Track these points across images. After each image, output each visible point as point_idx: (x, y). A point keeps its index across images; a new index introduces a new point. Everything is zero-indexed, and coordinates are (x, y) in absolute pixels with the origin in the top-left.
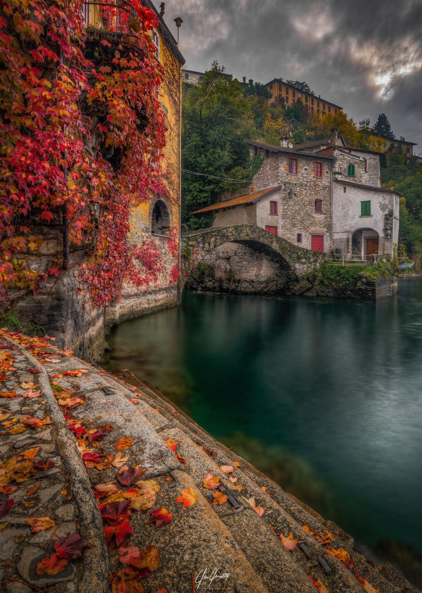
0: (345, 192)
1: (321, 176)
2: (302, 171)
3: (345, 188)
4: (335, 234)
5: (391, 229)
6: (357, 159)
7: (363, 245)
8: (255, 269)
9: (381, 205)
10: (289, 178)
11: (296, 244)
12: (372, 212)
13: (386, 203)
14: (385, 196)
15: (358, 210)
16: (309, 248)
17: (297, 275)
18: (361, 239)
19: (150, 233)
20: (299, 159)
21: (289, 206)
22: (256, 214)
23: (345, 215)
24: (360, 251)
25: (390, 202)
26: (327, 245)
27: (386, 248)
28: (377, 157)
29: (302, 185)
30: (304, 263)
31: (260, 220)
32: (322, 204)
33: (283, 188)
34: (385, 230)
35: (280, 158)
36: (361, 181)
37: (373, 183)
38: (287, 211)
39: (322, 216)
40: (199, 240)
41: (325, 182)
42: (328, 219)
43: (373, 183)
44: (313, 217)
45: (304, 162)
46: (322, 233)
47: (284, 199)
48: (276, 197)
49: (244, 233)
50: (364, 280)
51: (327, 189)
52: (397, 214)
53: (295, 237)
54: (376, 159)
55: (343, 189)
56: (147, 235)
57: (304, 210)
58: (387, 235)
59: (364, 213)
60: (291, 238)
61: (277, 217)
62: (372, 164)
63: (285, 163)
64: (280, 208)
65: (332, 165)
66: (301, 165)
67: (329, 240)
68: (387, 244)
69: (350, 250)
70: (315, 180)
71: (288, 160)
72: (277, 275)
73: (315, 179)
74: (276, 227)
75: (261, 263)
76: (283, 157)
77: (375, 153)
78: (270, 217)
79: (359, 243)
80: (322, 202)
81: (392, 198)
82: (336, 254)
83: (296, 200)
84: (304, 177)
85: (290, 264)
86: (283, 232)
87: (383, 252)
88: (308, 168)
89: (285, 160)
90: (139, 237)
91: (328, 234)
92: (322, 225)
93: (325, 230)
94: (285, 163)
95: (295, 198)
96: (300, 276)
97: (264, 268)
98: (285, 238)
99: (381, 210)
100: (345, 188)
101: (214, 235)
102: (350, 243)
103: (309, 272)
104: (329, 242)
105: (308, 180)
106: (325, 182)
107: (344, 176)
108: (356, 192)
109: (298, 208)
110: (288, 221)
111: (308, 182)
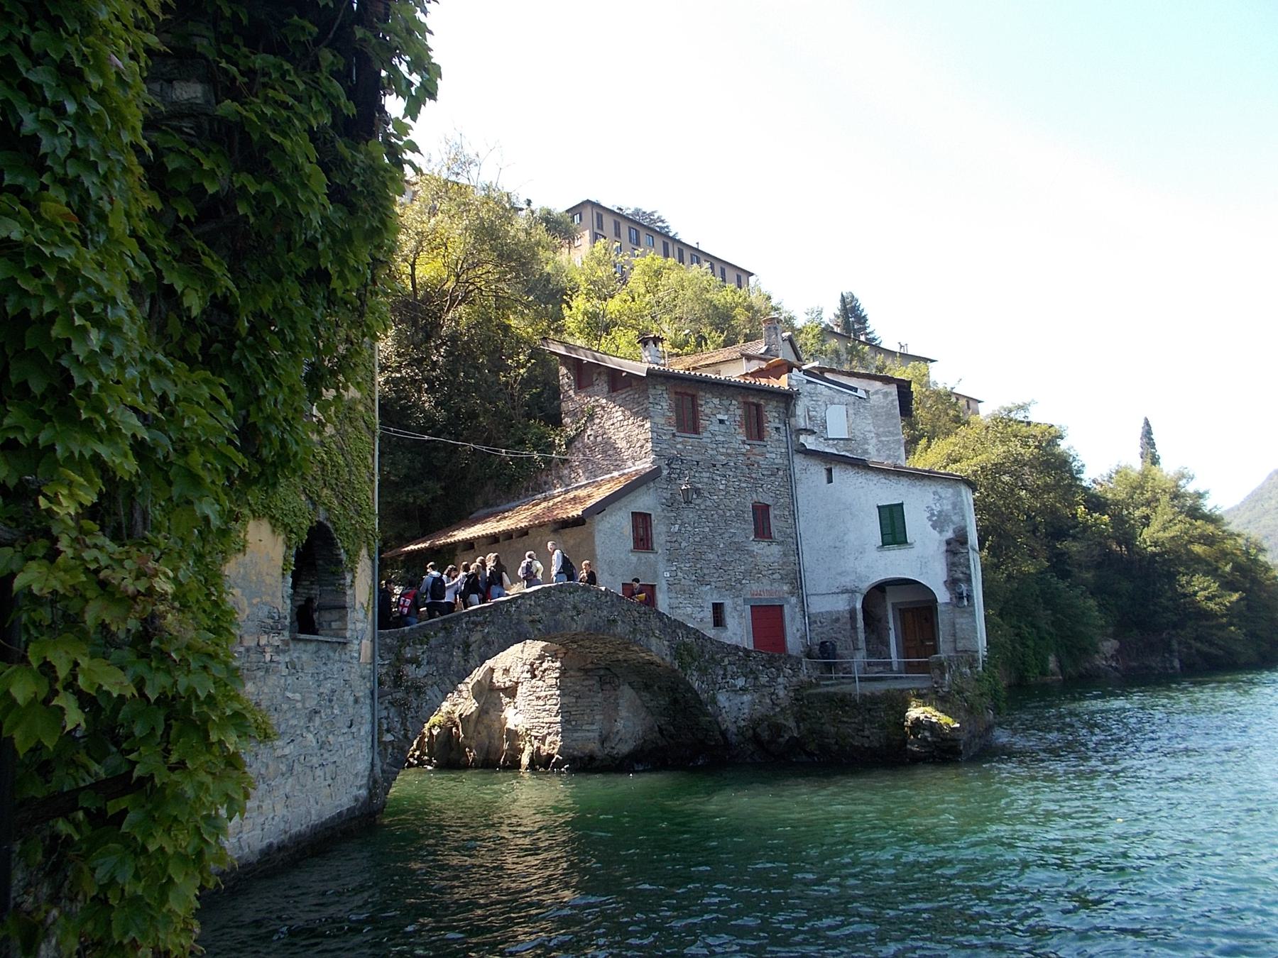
0: (830, 481)
1: (761, 438)
2: (711, 428)
3: (829, 471)
4: (812, 600)
5: (969, 580)
6: (850, 395)
7: (891, 625)
8: (597, 717)
9: (933, 515)
10: (679, 446)
11: (711, 632)
12: (911, 535)
13: (945, 508)
14: (939, 490)
15: (872, 529)
16: (748, 644)
17: (723, 727)
18: (886, 611)
19: (286, 633)
20: (702, 393)
21: (683, 524)
22: (594, 550)
23: (838, 544)
24: (888, 645)
25: (954, 506)
26: (794, 634)
27: (959, 634)
28: (893, 389)
29: (714, 466)
30: (744, 690)
31: (605, 567)
32: (771, 516)
33: (665, 472)
34: (952, 583)
35: (651, 391)
36: (865, 452)
37: (889, 457)
38: (680, 540)
39: (775, 549)
40: (433, 641)
41: (774, 456)
42: (792, 558)
43: (889, 457)
44: (750, 553)
45: (716, 401)
46: (780, 599)
47: (670, 504)
48: (644, 501)
49: (567, 610)
51: (781, 473)
52: (973, 538)
53: (708, 614)
54: (891, 393)
55: (824, 473)
56: (276, 641)
57: (726, 536)
58: (960, 597)
59: (889, 538)
60: (696, 615)
61: (651, 556)
62: (883, 407)
63: (664, 404)
64: (659, 532)
65: (787, 409)
66: (708, 411)
67: (799, 616)
68: (962, 621)
69: (862, 644)
70: (747, 450)
71: (673, 396)
72: (661, 730)
73: (748, 447)
74: (653, 587)
75: (616, 699)
76: (660, 389)
77: (888, 380)
78: (634, 558)
79: (879, 621)
80: (771, 510)
81: (959, 494)
82: (825, 654)
83: (703, 507)
84: (717, 443)
85: (704, 696)
86: (672, 601)
88: (725, 418)
89: (665, 396)
90: (248, 650)
91: (794, 600)
92: (776, 576)
93: (785, 588)
94: (664, 404)
95: (698, 501)
96: (733, 729)
97: (624, 713)
98: (678, 615)
99: (934, 527)
100: (829, 471)
101: (480, 623)
102: (860, 623)
103: (757, 715)
104: (798, 623)
105: (729, 451)
106: (774, 456)
107: (821, 439)
108: (860, 480)
109: (707, 529)
110: (685, 568)
111: (729, 455)
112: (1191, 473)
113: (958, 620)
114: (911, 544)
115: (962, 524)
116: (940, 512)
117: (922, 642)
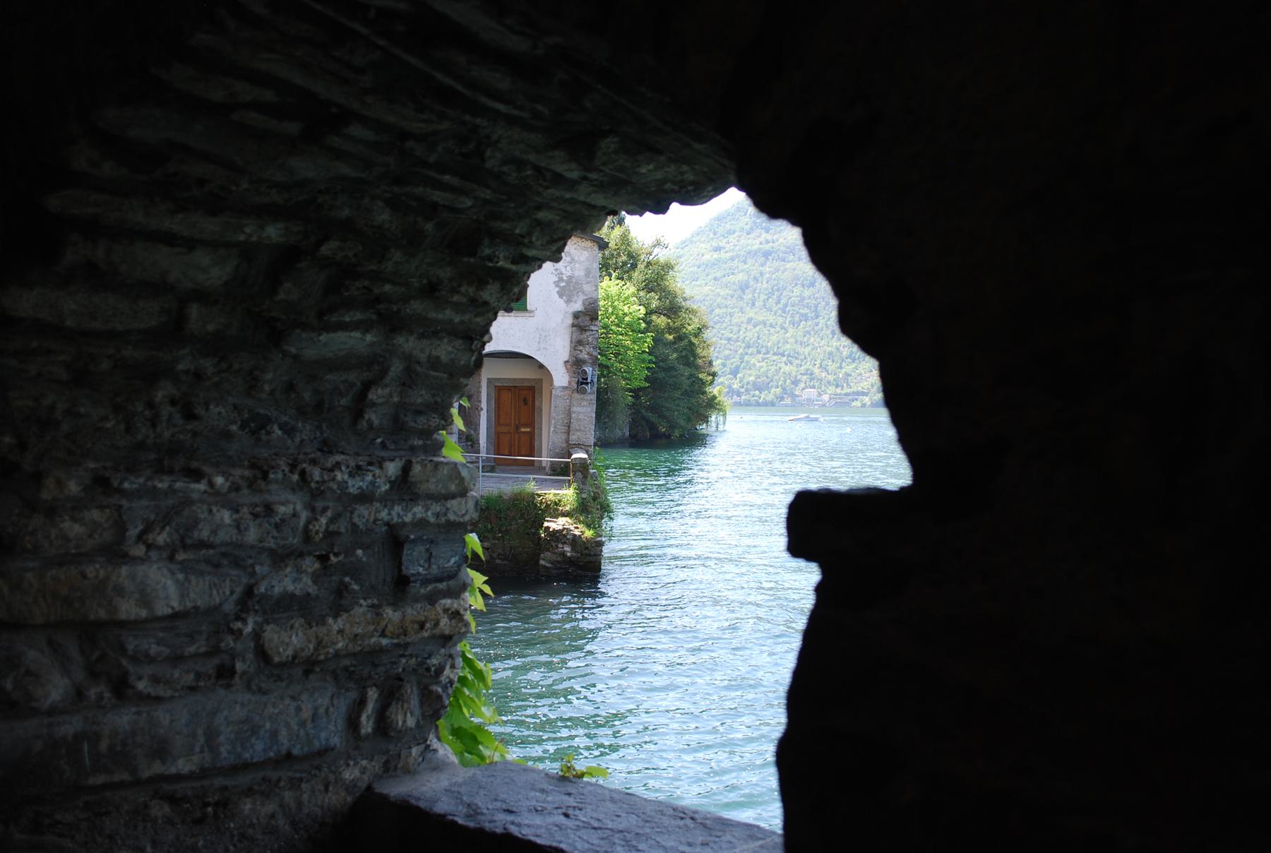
7: (484, 405)
9: (561, 280)
13: (577, 273)
18: (480, 387)
27: (574, 425)
50: (567, 548)
87: (564, 437)
99: (561, 295)
112: (666, 242)
113: (574, 409)
114: (532, 312)
115: (594, 296)
116: (570, 277)
117: (517, 427)
